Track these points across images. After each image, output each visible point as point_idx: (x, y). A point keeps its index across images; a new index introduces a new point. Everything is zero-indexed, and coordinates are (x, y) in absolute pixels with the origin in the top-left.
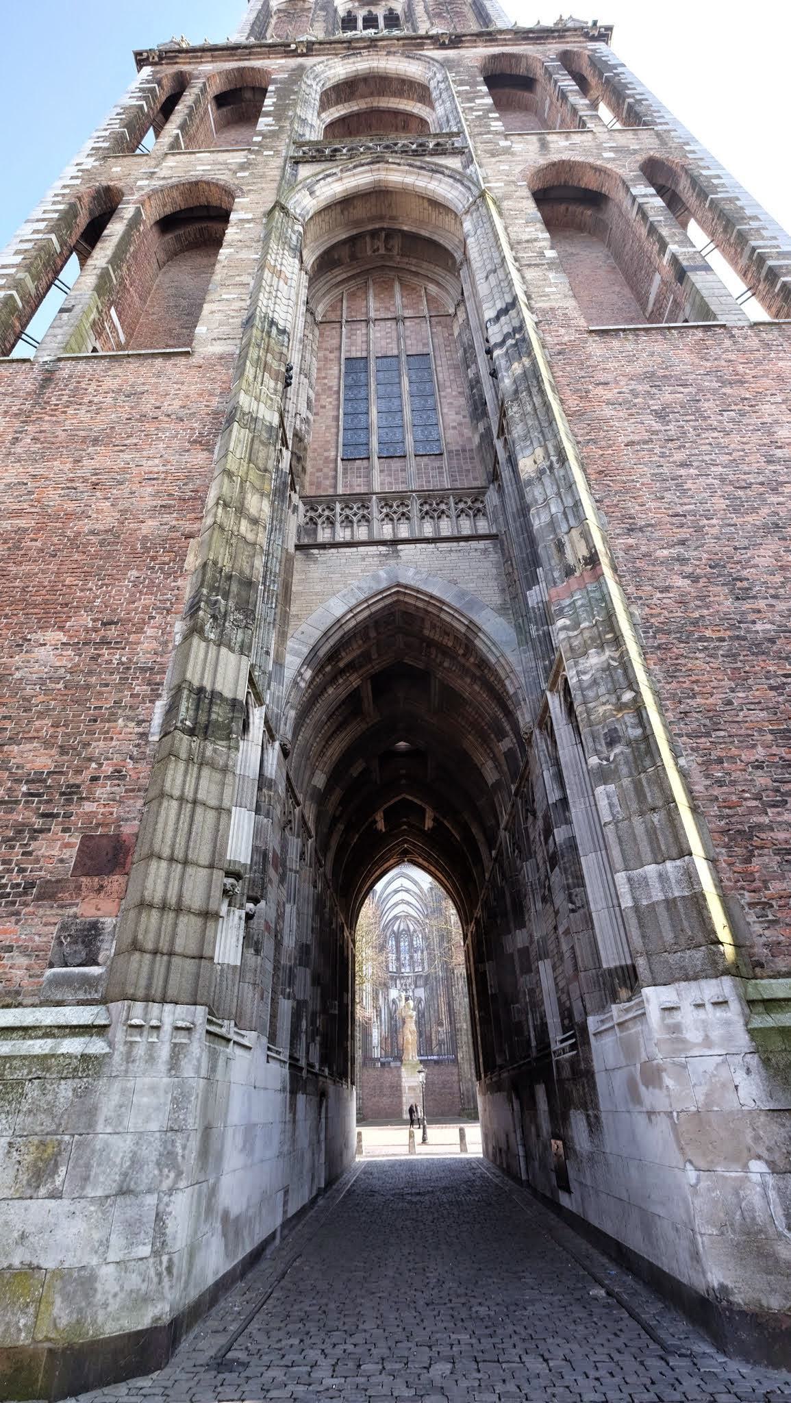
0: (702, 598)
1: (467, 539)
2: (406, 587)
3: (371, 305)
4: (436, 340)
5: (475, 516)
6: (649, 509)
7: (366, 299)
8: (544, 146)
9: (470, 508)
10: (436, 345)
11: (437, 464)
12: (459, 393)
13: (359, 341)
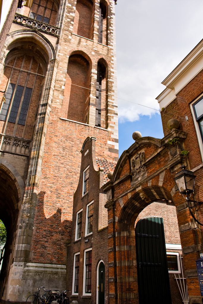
0: (51, 196)
1: (21, 155)
2: (3, 165)
3: (22, 65)
4: (36, 85)
5: (26, 148)
6: (51, 173)
7: (22, 61)
8: (79, 43)
9: (25, 145)
10: (36, 86)
11: (22, 128)
12: (36, 106)
13: (15, 78)
